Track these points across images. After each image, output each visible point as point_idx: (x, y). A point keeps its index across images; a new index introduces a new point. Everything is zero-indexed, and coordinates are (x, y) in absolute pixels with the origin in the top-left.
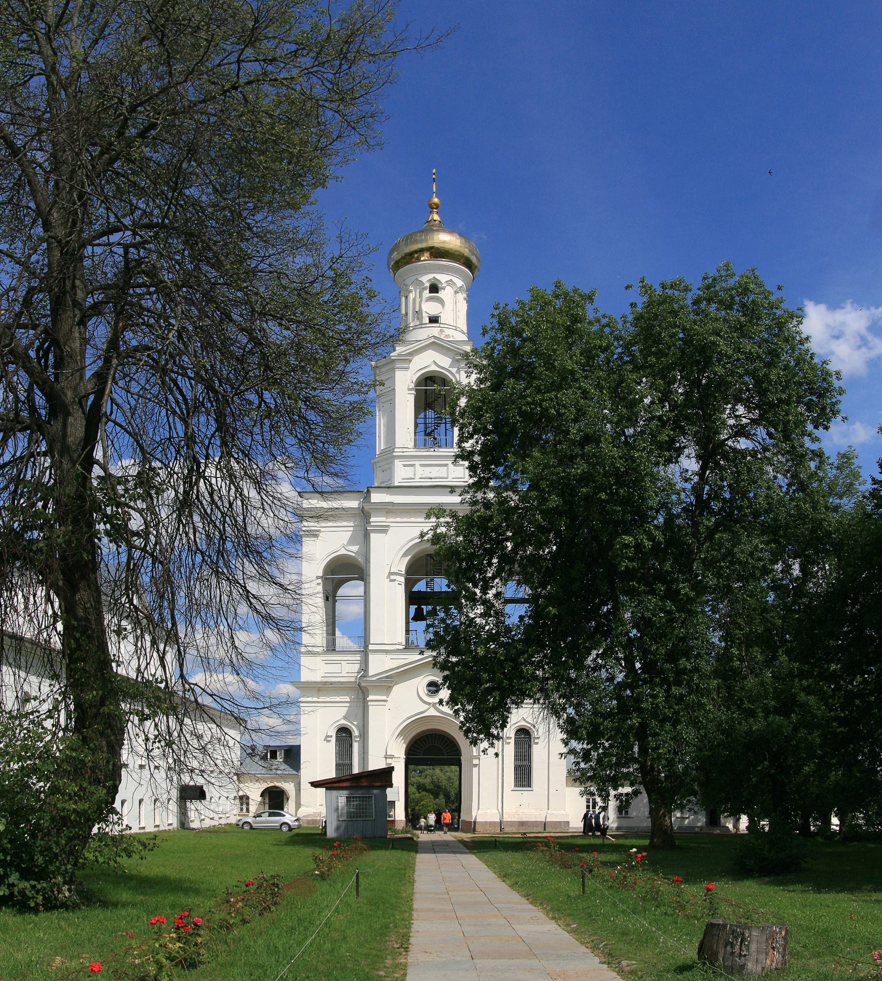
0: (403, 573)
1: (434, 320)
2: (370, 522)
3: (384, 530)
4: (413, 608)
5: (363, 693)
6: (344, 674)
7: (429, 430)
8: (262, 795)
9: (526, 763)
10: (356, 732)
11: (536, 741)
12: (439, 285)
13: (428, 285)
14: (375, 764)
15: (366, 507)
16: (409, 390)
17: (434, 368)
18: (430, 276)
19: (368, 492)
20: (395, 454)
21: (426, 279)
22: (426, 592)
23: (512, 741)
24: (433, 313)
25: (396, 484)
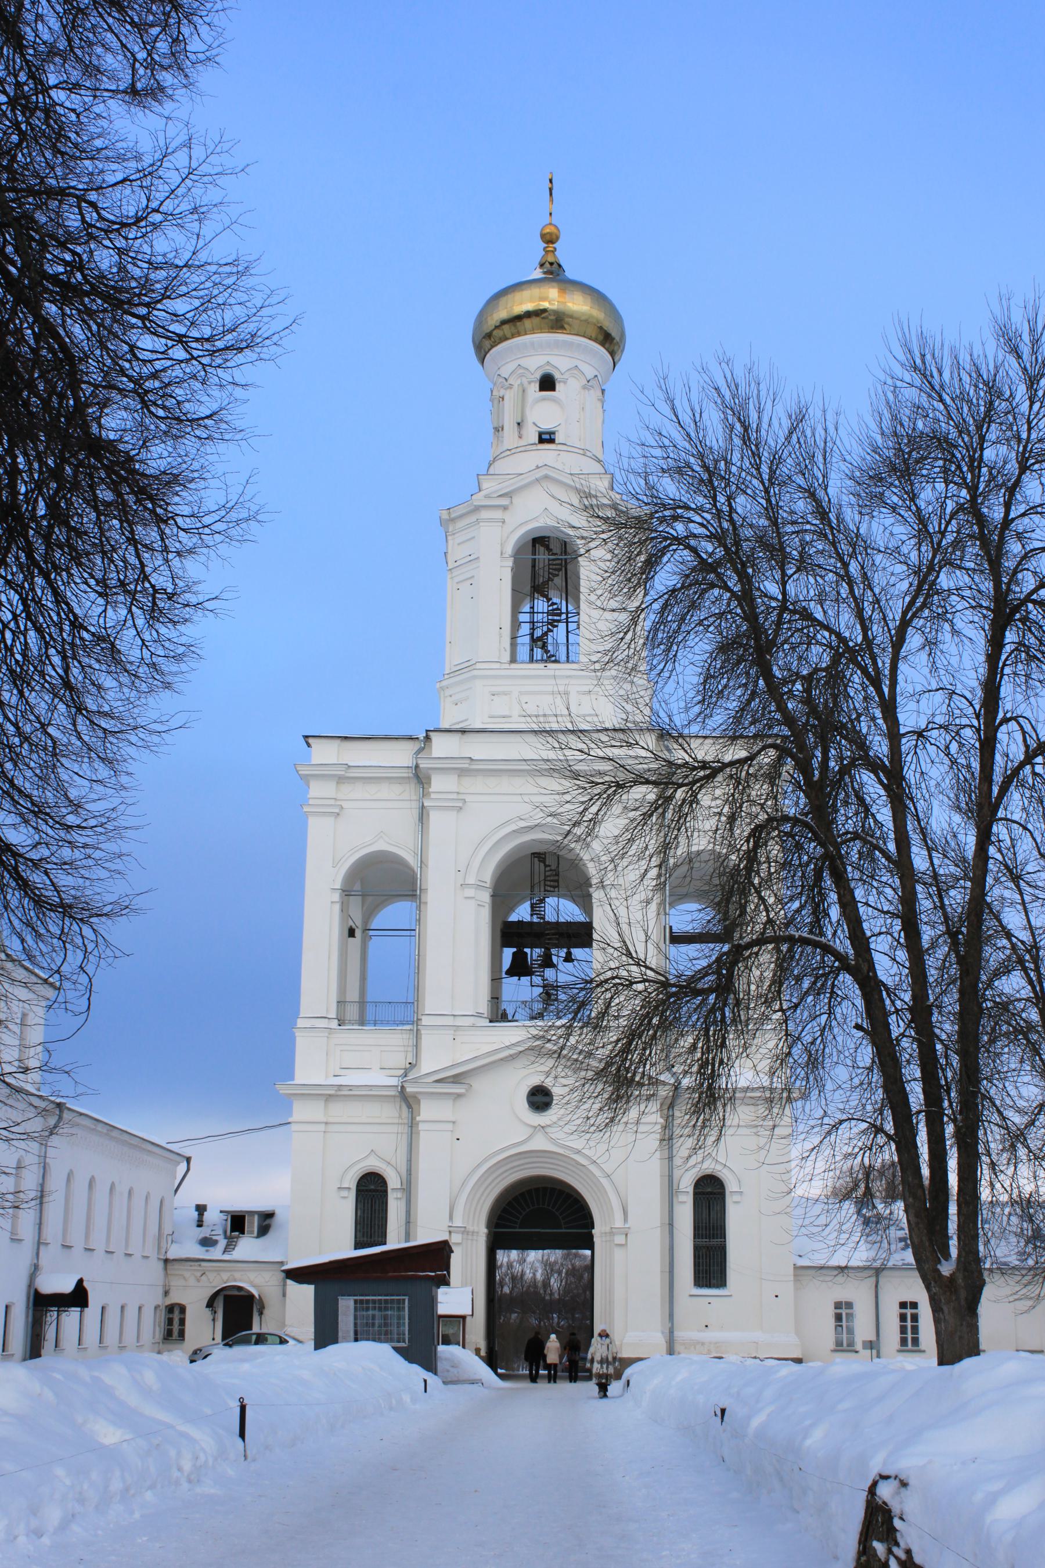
1: (546, 438)
2: (429, 794)
4: (508, 953)
5: (409, 1106)
7: (538, 633)
9: (715, 1242)
11: (736, 1198)
13: (538, 376)
14: (424, 1236)
15: (424, 764)
22: (531, 923)
24: (546, 426)
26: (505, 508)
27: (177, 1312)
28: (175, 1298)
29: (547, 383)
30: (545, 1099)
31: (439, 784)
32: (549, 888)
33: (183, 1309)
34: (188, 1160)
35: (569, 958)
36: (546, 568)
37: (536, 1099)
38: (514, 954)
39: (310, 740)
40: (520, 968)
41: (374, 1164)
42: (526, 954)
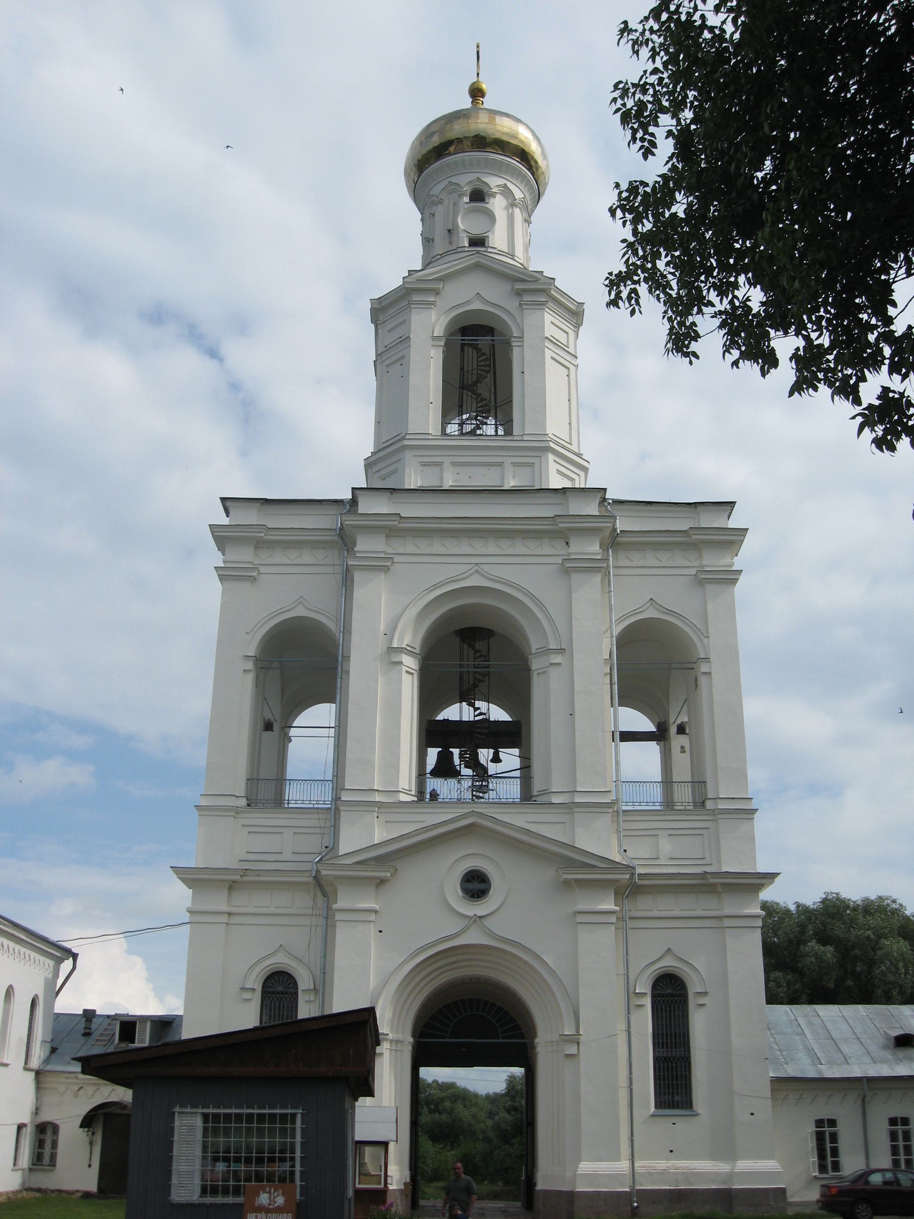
0: (417, 651)
2: (355, 553)
3: (382, 566)
4: (433, 754)
6: (287, 855)
8: (88, 1122)
10: (304, 982)
12: (485, 190)
13: (468, 189)
16: (434, 338)
17: (477, 306)
18: (473, 177)
19: (354, 502)
20: (406, 443)
21: (466, 181)
23: (648, 1002)
25: (407, 487)
26: (437, 292)
27: (49, 1132)
28: (45, 1117)
29: (478, 196)
30: (482, 886)
31: (366, 545)
32: (478, 676)
33: (55, 1128)
34: (75, 956)
35: (496, 759)
36: (475, 372)
37: (471, 886)
38: (439, 753)
39: (228, 504)
40: (445, 769)
41: (282, 961)
42: (452, 753)
